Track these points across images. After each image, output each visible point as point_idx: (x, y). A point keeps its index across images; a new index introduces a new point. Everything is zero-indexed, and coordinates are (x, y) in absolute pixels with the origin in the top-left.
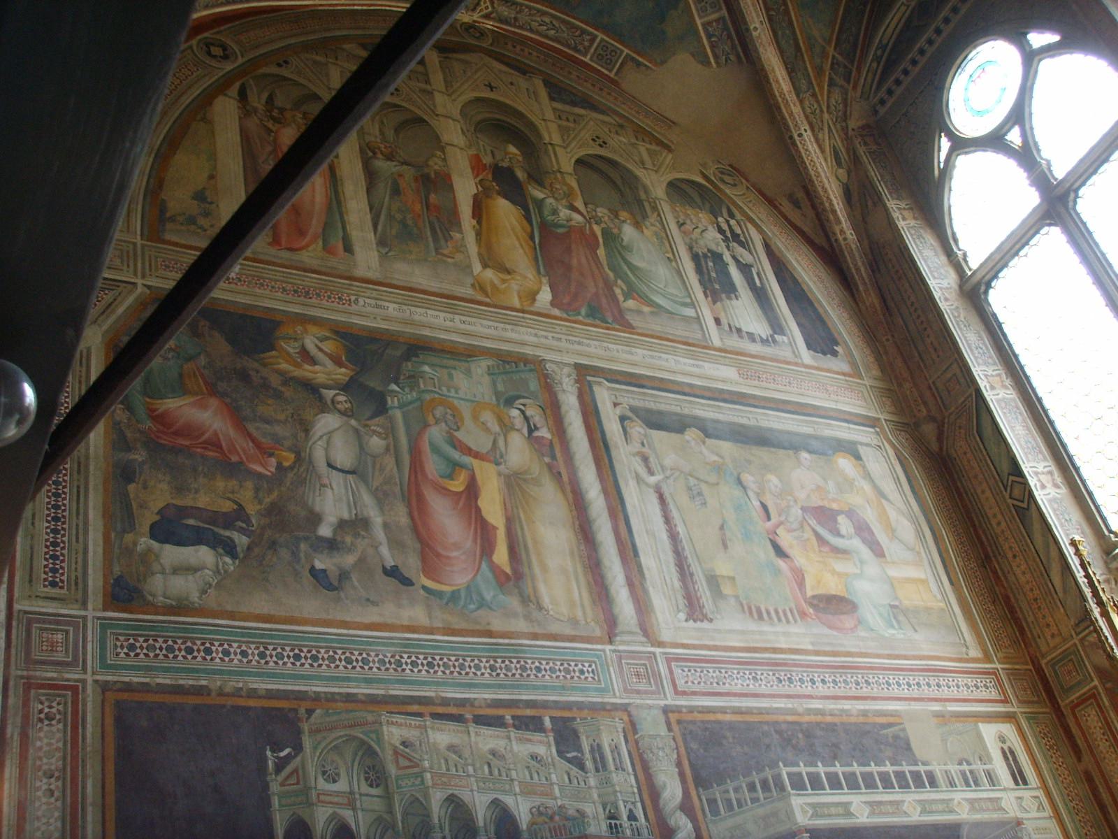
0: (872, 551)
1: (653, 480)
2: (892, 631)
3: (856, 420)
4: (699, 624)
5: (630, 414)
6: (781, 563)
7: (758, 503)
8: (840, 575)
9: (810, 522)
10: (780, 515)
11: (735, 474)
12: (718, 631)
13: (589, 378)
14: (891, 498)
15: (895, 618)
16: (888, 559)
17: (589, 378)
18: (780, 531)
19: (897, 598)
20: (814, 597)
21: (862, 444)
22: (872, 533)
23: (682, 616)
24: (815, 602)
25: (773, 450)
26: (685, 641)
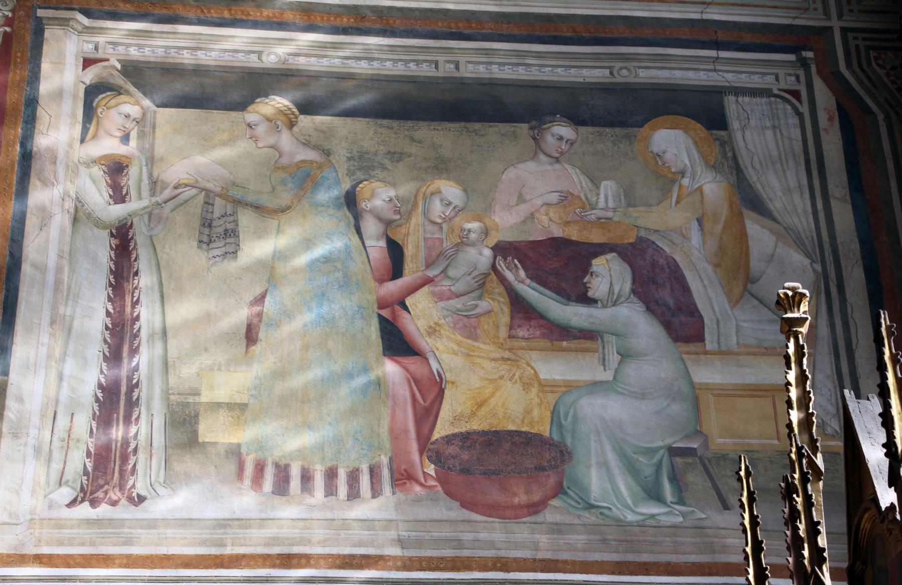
0: (667, 326)
1: (118, 211)
2: (655, 509)
3: (747, 38)
4: (103, 510)
5: (120, 80)
6: (391, 369)
7: (383, 243)
8: (546, 387)
9: (509, 275)
10: (428, 266)
11: (347, 185)
12: (151, 524)
13: (41, 13)
14: (777, 205)
15: (674, 479)
16: (710, 343)
17: (41, 13)
18: (419, 302)
19: (698, 433)
20: (448, 440)
21: (739, 91)
22: (686, 289)
23: (66, 494)
24: (452, 450)
25: (477, 126)
26: (45, 550)
